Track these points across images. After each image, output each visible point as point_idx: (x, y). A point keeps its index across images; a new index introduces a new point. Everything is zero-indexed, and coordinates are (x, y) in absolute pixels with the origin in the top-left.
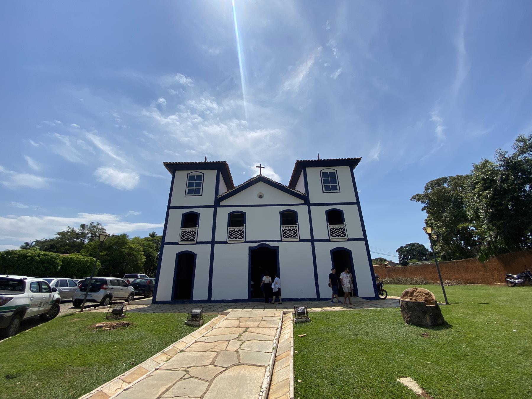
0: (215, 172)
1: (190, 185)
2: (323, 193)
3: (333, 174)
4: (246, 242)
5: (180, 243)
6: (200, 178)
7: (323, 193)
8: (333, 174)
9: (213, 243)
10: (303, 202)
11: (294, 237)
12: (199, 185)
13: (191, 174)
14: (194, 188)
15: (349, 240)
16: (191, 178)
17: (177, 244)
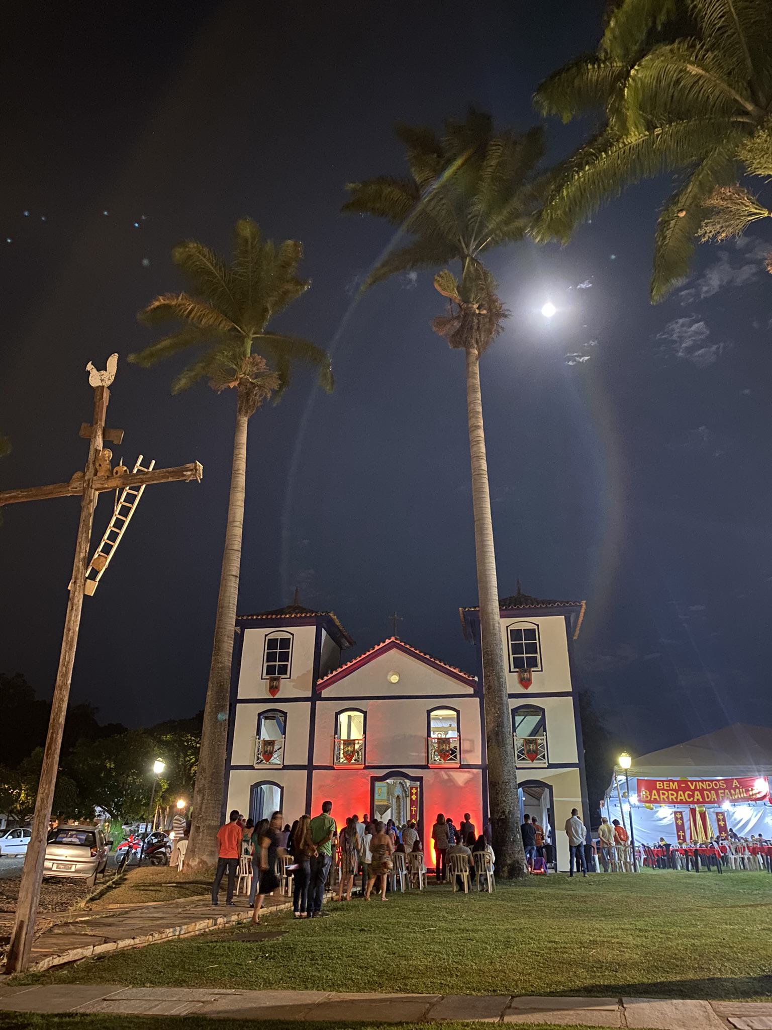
0: (313, 629)
1: (270, 657)
2: (510, 672)
3: (531, 634)
4: (366, 768)
5: (256, 766)
6: (285, 643)
7: (510, 672)
8: (531, 634)
9: (310, 767)
10: (471, 691)
11: (451, 759)
12: (285, 657)
13: (271, 637)
14: (277, 663)
15: (551, 766)
16: (272, 644)
17: (251, 767)
